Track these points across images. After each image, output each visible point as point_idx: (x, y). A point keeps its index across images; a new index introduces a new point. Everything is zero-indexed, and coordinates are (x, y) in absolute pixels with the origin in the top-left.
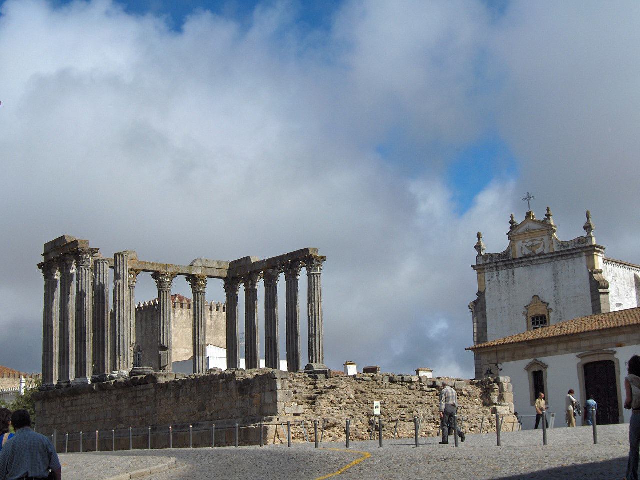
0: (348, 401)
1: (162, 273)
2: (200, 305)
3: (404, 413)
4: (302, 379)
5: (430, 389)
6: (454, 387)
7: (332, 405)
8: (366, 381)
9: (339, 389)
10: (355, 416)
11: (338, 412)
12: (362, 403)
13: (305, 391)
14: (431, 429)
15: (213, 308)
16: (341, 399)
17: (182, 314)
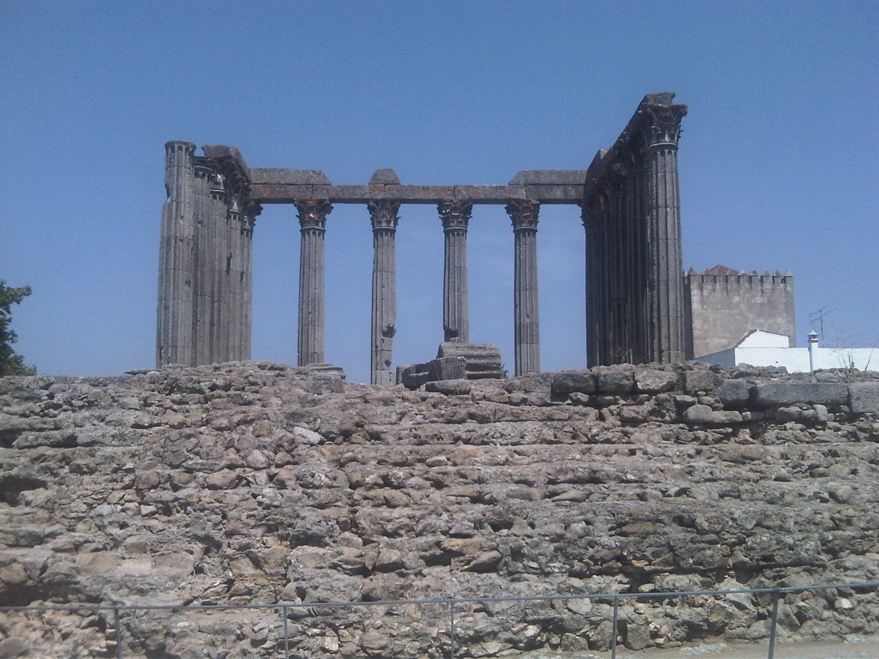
0: (216, 478)
1: (446, 201)
2: (523, 252)
3: (466, 526)
4: (200, 391)
5: (736, 416)
6: (848, 403)
7: (130, 494)
8: (447, 392)
9: (202, 429)
10: (225, 541)
11: (153, 523)
12: (290, 483)
13: (121, 438)
14: (584, 606)
15: (764, 278)
16: (189, 471)
17: (714, 290)
